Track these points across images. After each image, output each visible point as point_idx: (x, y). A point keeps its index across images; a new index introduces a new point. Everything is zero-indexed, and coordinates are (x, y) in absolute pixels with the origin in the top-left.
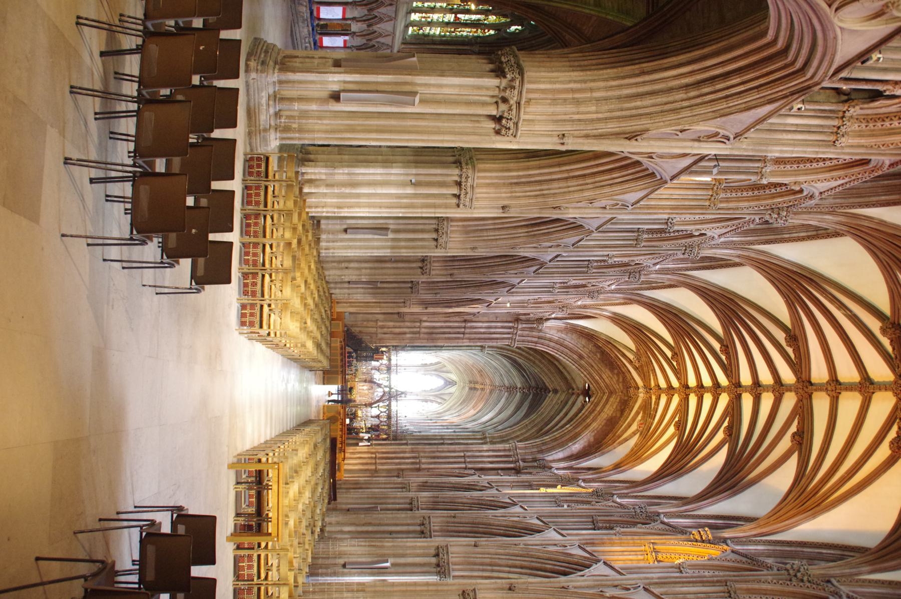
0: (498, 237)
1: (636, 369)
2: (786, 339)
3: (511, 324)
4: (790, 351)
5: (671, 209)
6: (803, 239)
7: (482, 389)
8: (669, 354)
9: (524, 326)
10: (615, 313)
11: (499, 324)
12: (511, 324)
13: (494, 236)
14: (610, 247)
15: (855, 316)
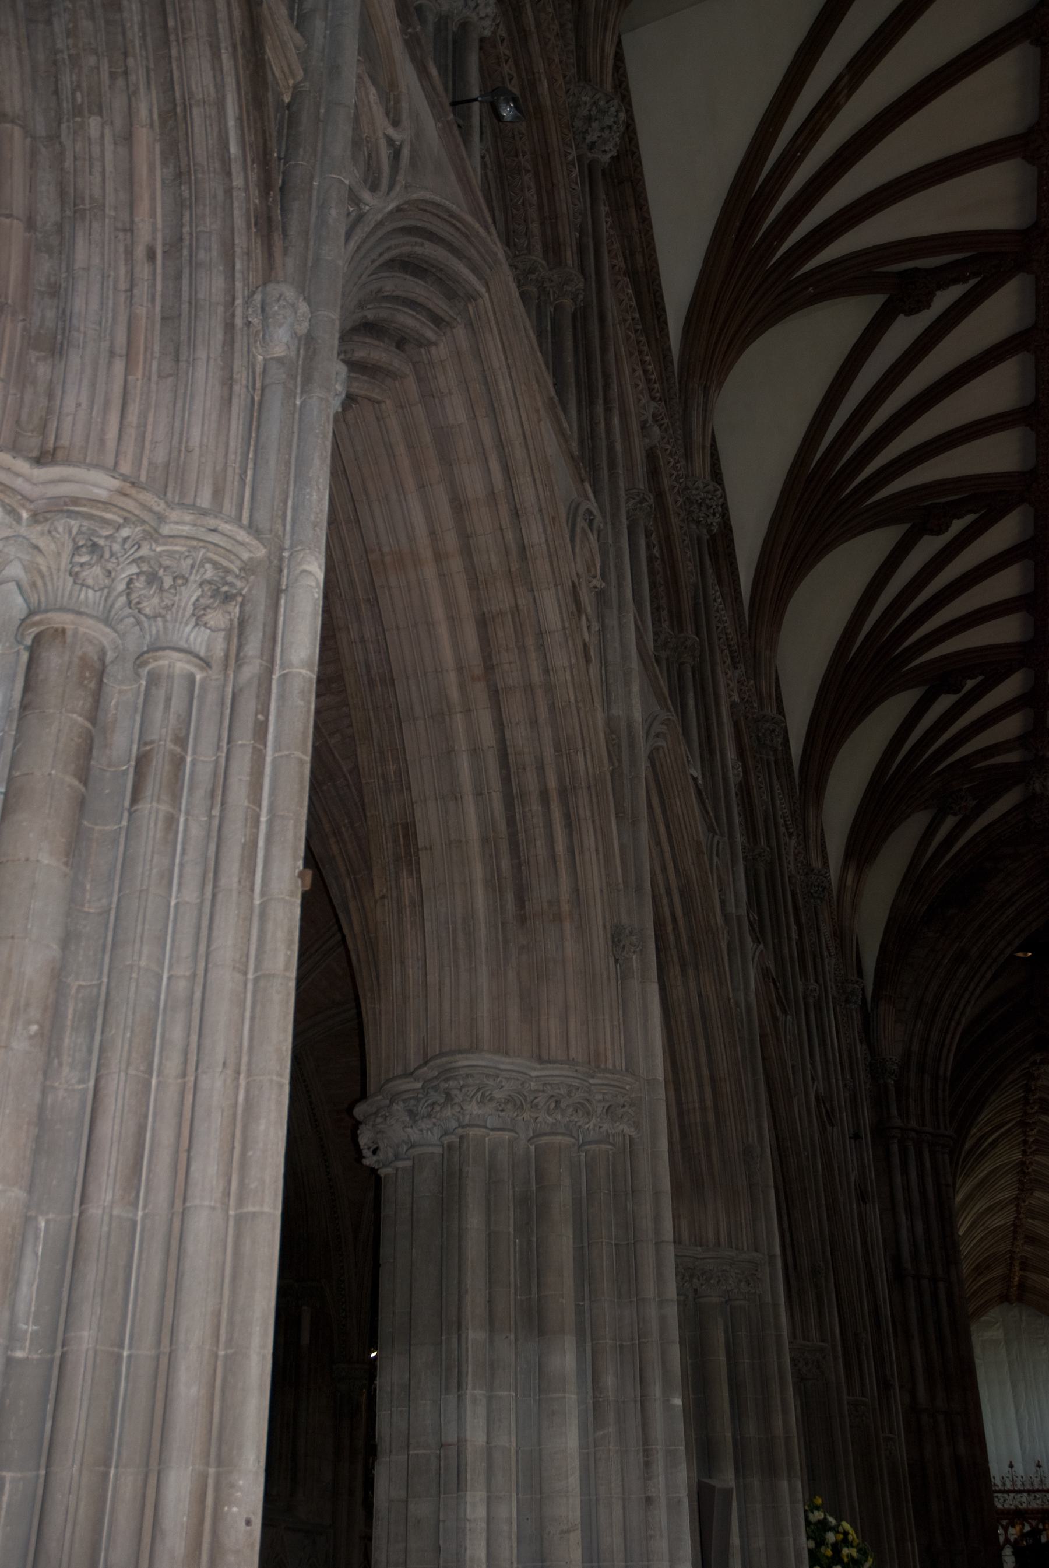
0: (705, 1072)
1: (980, 809)
2: (910, 312)
3: (895, 1148)
4: (944, 299)
5: (592, 403)
6: (646, 221)
7: (1024, 1266)
8: (944, 702)
9: (894, 1112)
10: (848, 856)
11: (898, 1180)
12: (895, 1148)
13: (701, 1086)
14: (708, 729)
15: (850, 65)
